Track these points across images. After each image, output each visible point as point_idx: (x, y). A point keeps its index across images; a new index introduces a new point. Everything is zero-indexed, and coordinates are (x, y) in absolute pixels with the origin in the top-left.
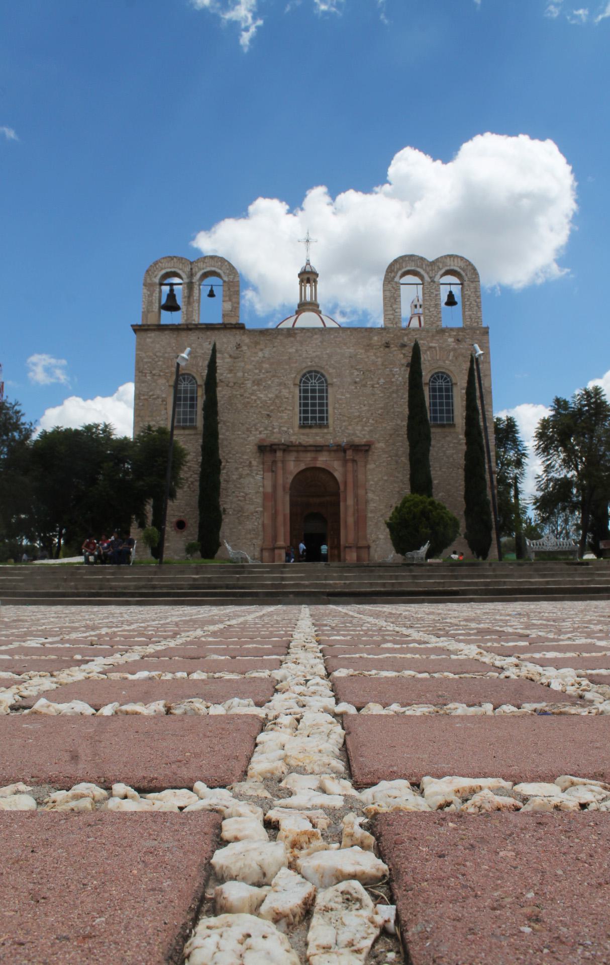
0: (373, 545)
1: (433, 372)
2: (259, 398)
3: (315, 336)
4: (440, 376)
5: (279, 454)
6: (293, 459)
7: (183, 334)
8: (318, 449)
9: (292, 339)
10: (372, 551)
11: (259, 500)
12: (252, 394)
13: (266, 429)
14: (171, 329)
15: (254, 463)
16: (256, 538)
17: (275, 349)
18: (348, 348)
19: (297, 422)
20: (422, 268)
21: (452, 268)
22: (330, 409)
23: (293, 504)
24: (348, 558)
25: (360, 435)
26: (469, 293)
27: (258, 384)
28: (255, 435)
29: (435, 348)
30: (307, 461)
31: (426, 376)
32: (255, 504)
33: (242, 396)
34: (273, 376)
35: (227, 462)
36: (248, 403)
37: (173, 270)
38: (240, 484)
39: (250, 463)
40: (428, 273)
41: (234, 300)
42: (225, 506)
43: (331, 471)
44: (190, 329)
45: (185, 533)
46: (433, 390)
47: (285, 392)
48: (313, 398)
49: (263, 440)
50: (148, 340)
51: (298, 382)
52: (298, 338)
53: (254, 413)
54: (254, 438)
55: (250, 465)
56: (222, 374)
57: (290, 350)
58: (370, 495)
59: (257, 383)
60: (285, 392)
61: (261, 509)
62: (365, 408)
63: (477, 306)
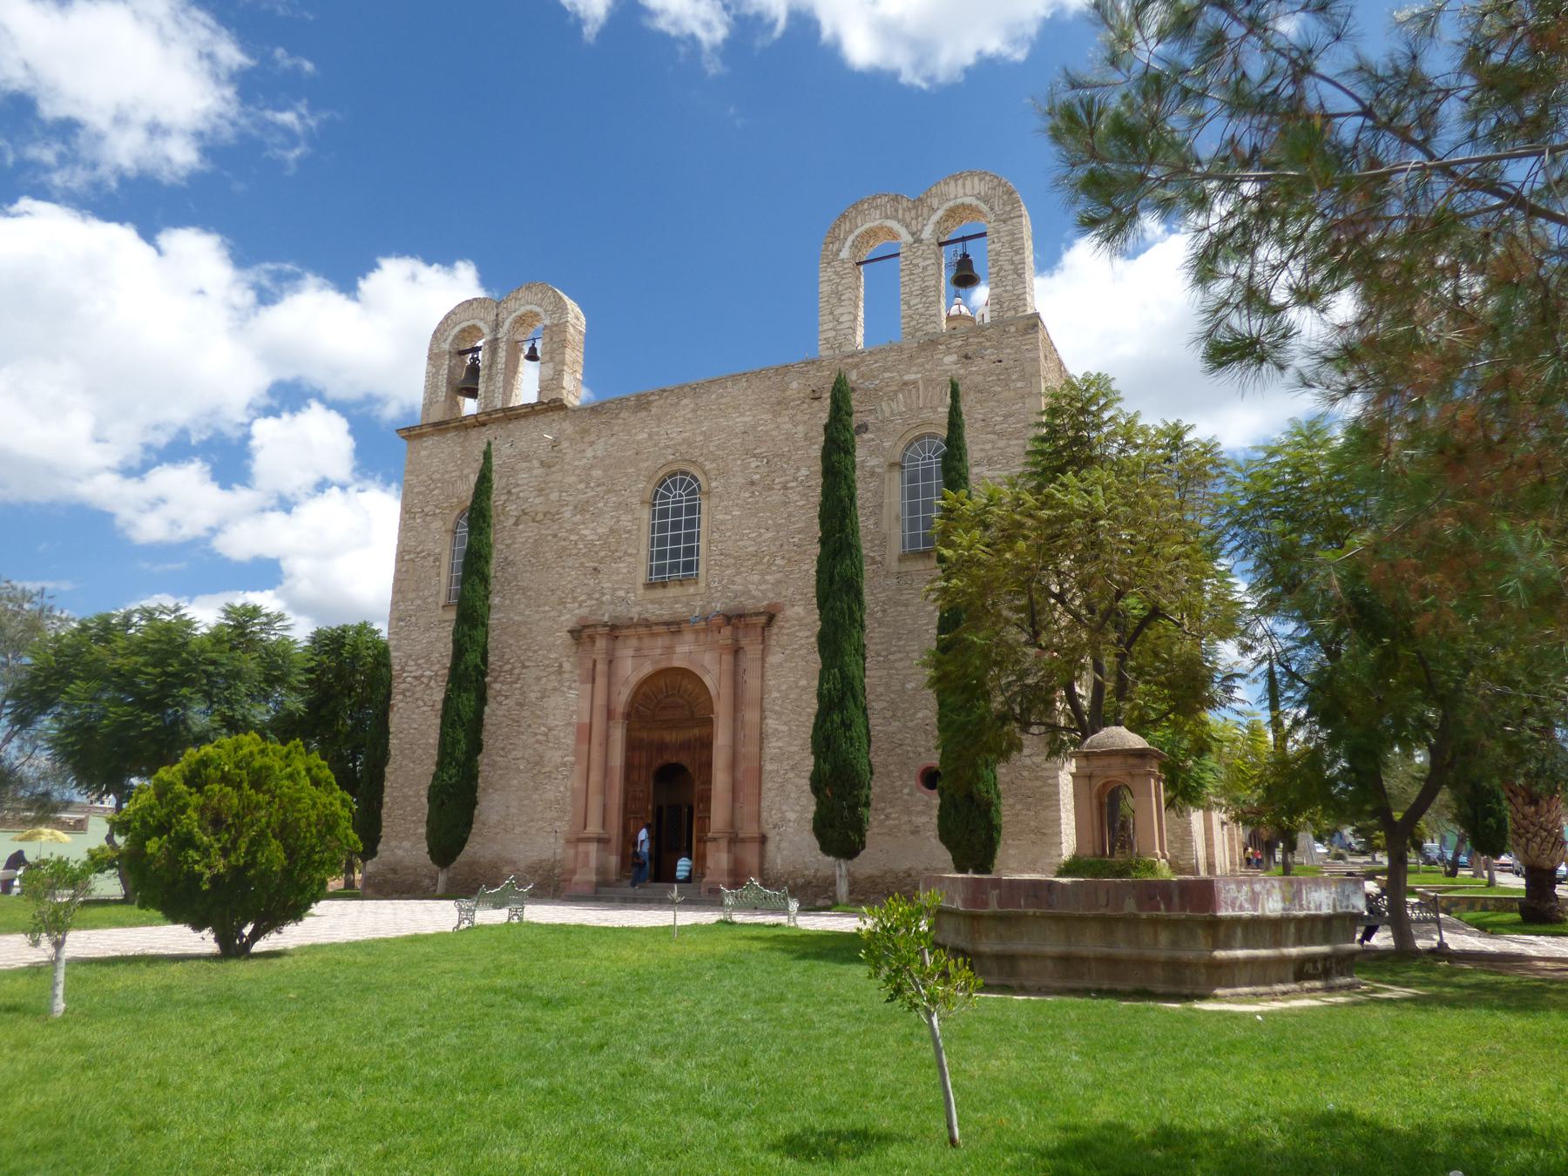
0: (771, 834)
1: (910, 436)
2: (583, 538)
3: (685, 401)
5: (601, 644)
6: (631, 652)
7: (473, 433)
8: (674, 627)
9: (644, 414)
10: (771, 847)
11: (570, 741)
12: (570, 531)
14: (456, 428)
15: (567, 666)
16: (558, 819)
17: (613, 440)
18: (742, 415)
19: (642, 576)
20: (895, 218)
21: (959, 201)
22: (703, 544)
23: (632, 745)
24: (710, 863)
25: (755, 589)
26: (997, 246)
27: (583, 511)
29: (915, 383)
32: (562, 752)
33: (555, 536)
35: (524, 667)
36: (564, 549)
39: (561, 666)
41: (558, 358)
44: (484, 424)
48: (676, 526)
49: (583, 618)
50: (423, 453)
51: (648, 495)
52: (654, 410)
54: (568, 619)
55: (560, 671)
57: (639, 437)
58: (771, 723)
59: (581, 508)
61: (572, 759)
62: (769, 535)
63: (1016, 271)
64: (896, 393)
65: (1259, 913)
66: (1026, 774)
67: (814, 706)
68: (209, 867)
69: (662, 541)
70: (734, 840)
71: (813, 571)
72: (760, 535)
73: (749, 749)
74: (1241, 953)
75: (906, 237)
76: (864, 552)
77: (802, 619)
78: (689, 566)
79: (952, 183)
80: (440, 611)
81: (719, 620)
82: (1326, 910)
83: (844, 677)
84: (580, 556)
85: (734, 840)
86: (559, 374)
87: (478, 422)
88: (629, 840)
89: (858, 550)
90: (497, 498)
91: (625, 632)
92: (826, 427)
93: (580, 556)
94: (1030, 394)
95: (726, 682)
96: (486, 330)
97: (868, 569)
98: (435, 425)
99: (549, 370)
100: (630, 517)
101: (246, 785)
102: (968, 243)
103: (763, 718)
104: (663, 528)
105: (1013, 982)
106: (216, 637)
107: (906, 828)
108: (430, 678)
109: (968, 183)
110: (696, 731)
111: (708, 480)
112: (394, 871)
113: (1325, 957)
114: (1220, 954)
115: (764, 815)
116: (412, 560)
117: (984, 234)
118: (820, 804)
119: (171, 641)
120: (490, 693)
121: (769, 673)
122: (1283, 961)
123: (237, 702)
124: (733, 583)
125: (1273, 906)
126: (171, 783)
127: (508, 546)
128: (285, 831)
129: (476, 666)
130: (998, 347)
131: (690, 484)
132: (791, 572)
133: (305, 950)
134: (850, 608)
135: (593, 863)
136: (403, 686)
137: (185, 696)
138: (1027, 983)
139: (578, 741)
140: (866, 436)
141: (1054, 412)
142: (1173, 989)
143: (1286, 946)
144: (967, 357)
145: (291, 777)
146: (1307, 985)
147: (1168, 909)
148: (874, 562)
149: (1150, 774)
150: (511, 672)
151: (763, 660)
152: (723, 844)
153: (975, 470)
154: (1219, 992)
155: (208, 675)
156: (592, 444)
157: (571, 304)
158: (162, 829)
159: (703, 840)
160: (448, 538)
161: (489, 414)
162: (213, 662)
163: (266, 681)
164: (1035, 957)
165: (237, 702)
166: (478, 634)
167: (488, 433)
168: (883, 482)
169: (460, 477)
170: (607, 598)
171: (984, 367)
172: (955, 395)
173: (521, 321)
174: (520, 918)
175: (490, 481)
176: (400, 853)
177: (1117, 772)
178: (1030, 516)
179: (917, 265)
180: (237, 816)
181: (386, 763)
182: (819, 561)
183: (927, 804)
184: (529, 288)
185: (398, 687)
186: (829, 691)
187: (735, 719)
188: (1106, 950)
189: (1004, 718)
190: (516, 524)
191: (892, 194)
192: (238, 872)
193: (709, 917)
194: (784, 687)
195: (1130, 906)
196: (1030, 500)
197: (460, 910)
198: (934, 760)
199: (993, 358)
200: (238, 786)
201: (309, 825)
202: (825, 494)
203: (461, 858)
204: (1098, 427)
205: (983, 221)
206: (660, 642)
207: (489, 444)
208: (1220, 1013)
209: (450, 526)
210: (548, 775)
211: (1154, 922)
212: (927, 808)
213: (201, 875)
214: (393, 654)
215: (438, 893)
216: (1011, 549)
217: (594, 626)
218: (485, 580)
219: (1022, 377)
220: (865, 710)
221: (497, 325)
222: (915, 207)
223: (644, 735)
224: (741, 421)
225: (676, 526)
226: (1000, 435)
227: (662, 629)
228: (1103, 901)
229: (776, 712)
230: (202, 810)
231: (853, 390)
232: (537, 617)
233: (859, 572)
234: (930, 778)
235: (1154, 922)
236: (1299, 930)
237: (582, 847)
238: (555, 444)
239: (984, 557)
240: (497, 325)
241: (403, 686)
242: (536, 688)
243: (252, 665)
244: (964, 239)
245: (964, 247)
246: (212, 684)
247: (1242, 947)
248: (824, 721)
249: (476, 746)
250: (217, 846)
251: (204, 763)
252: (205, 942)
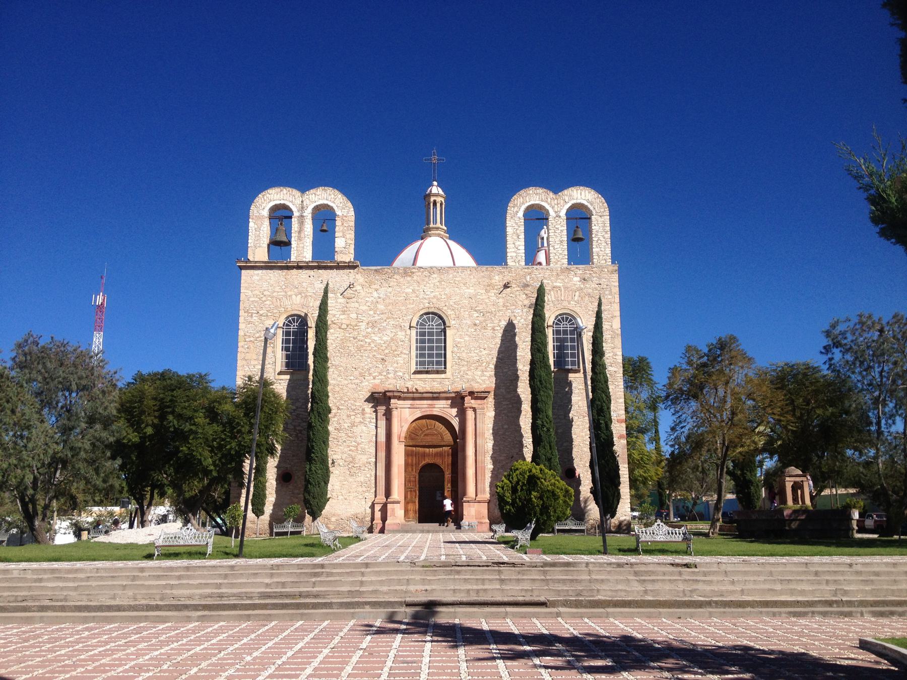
2: (373, 341)
3: (434, 276)
4: (566, 317)
7: (294, 271)
8: (435, 396)
9: (409, 278)
12: (366, 337)
13: (380, 374)
17: (390, 289)
27: (373, 327)
28: (368, 381)
30: (425, 407)
31: (550, 316)
35: (339, 409)
36: (362, 346)
37: (282, 202)
39: (363, 410)
42: (335, 457)
45: (291, 487)
46: (557, 332)
47: (401, 335)
49: (376, 385)
51: (414, 324)
52: (415, 278)
53: (368, 357)
56: (334, 316)
59: (373, 324)
62: (484, 352)
100: (403, 333)
130: (600, 278)
232: (346, 382)
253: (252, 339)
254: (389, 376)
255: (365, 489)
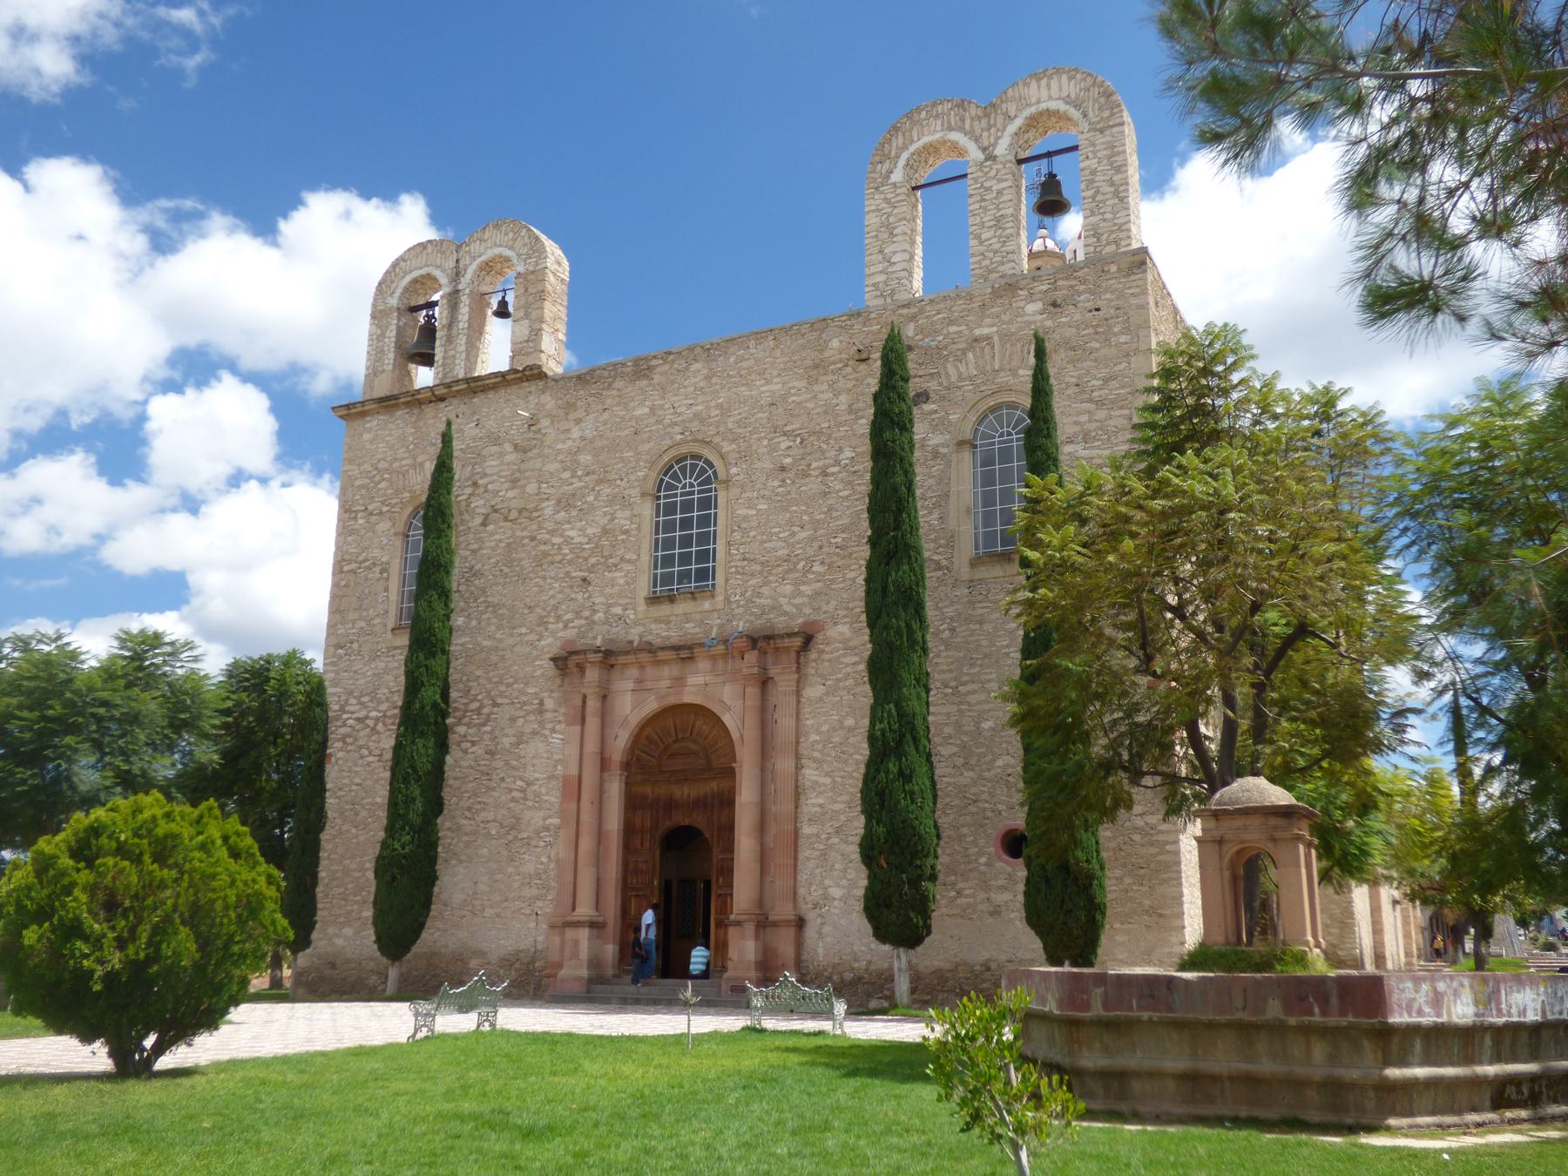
0: (811, 916)
1: (983, 406)
2: (568, 540)
5: (592, 675)
6: (631, 685)
7: (429, 410)
8: (685, 652)
9: (644, 383)
10: (810, 932)
11: (554, 798)
12: (552, 532)
13: (578, 615)
14: (407, 404)
15: (549, 704)
17: (606, 416)
18: (768, 382)
19: (643, 588)
20: (961, 129)
21: (1043, 106)
22: (720, 546)
23: (632, 803)
24: (733, 953)
25: (787, 603)
26: (1092, 163)
28: (553, 633)
29: (988, 338)
32: (544, 812)
33: (533, 539)
34: (600, 482)
35: (495, 705)
36: (545, 554)
38: (519, 758)
39: (541, 703)
40: (976, 141)
41: (534, 314)
43: (715, 708)
44: (442, 399)
47: (623, 518)
48: (687, 524)
50: (367, 436)
51: (650, 486)
53: (556, 579)
54: (551, 644)
55: (541, 711)
57: (638, 412)
58: (810, 774)
59: (564, 503)
60: (623, 518)
61: (556, 821)
62: (804, 534)
63: (1116, 194)
64: (964, 351)
65: (1444, 1019)
66: (1137, 837)
67: (861, 752)
68: (101, 962)
69: (668, 544)
70: (763, 924)
71: (861, 580)
72: (793, 534)
73: (783, 807)
74: (1421, 1072)
75: (975, 154)
76: (926, 554)
77: (847, 640)
78: (703, 575)
79: (1034, 84)
80: (389, 635)
81: (742, 643)
82: (1532, 1017)
83: (902, 714)
84: (565, 564)
85: (763, 924)
86: (536, 334)
87: (435, 396)
88: (630, 923)
89: (919, 553)
90: (460, 492)
91: (622, 659)
92: (876, 397)
93: (565, 564)
94: (1137, 351)
95: (752, 722)
96: (443, 280)
97: (931, 576)
98: (381, 400)
99: (524, 329)
100: (628, 513)
101: (147, 858)
102: (1055, 159)
103: (799, 768)
104: (669, 526)
105: (1124, 1107)
106: (108, 672)
107: (982, 909)
108: (377, 719)
109: (1054, 84)
110: (714, 785)
111: (727, 465)
112: (333, 965)
113: (1533, 1078)
114: (1393, 1072)
115: (802, 891)
116: (353, 571)
117: (1075, 148)
118: (872, 877)
119: (52, 677)
120: (453, 738)
121: (806, 710)
122: (1477, 1082)
123: (135, 752)
124: (759, 595)
125: (1462, 1011)
126: (54, 857)
127: (474, 551)
128: (196, 915)
129: (435, 705)
130: (1095, 292)
131: (703, 471)
132: (833, 581)
133: (221, 1067)
134: (908, 626)
135: (584, 953)
136: (342, 731)
137: (69, 747)
138: (1142, 1109)
139: (565, 796)
140: (927, 407)
141: (1168, 374)
142: (1331, 1118)
143: (1481, 1063)
144: (1055, 305)
145: (203, 847)
146: (1509, 1114)
147: (1324, 1013)
148: (939, 567)
149: (1299, 838)
150: (478, 712)
151: (798, 694)
152: (750, 929)
153: (1067, 449)
154: (1392, 1122)
155: (99, 719)
156: (578, 421)
157: (550, 246)
158: (42, 914)
159: (723, 925)
160: (398, 542)
161: (448, 386)
162: (104, 703)
163: (171, 725)
164: (1154, 1075)
165: (135, 752)
166: (436, 663)
167: (447, 410)
168: (948, 464)
169: (413, 466)
170: (599, 616)
171: (1077, 317)
172: (1040, 353)
173: (488, 268)
174: (493, 1025)
175: (450, 470)
176: (339, 942)
177: (1254, 834)
178: (1140, 507)
179: (989, 189)
180: (136, 897)
181: (322, 829)
182: (868, 567)
183: (1010, 877)
184: (497, 226)
185: (336, 732)
186: (883, 731)
187: (763, 769)
188: (1244, 1067)
189: (1108, 766)
190: (484, 524)
191: (957, 100)
192: (137, 968)
193: (732, 1023)
194: (825, 728)
195: (1274, 1009)
196: (1139, 488)
197: (417, 1015)
198: (1019, 820)
199: (1089, 305)
200: (138, 860)
201: (226, 908)
202: (876, 482)
203: (417, 948)
204: (1225, 392)
205: (1074, 132)
206: (666, 671)
207: (449, 424)
208: (1395, 1149)
209: (401, 527)
210: (527, 842)
211: (1307, 1030)
212: (1010, 881)
213: (92, 972)
214: (330, 690)
215: (388, 993)
216: (1115, 550)
217: (584, 652)
218: (445, 595)
219: (1127, 330)
220: (929, 756)
221: (457, 275)
222: (987, 115)
223: (648, 790)
224: (767, 389)
225: (687, 524)
226: (1100, 403)
227: (670, 655)
228: (1239, 1003)
229: (815, 760)
230: (92, 890)
231: (910, 348)
232: (511, 641)
233: (920, 580)
234: (1014, 844)
235: (1307, 1030)
236: (1497, 1043)
237: (570, 933)
238: (532, 423)
239: (1080, 559)
240: (457, 275)
241: (342, 731)
242: (509, 731)
243: (153, 706)
244: (1049, 155)
245: (1050, 165)
246: (105, 731)
247: (1422, 1064)
248: (878, 771)
249: (436, 806)
250: (111, 935)
251: (96, 831)
252: (95, 1057)
253: (353, 566)
254: (596, 617)
255: (535, 892)
